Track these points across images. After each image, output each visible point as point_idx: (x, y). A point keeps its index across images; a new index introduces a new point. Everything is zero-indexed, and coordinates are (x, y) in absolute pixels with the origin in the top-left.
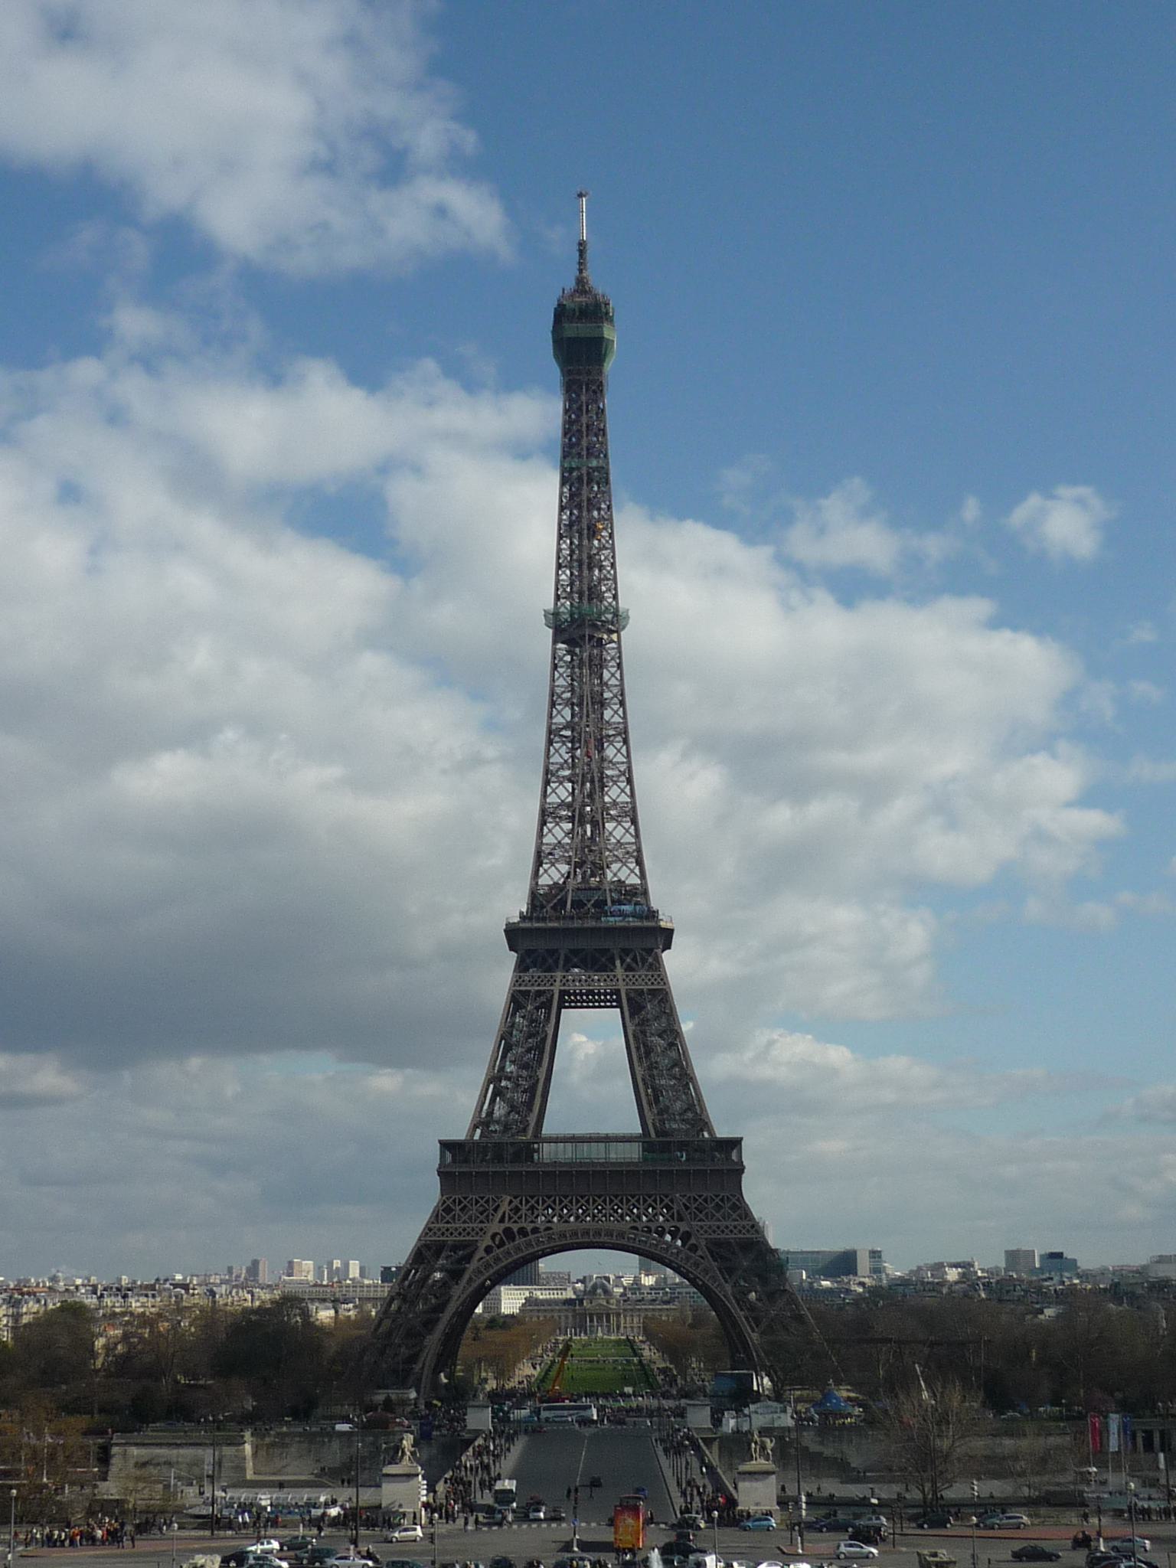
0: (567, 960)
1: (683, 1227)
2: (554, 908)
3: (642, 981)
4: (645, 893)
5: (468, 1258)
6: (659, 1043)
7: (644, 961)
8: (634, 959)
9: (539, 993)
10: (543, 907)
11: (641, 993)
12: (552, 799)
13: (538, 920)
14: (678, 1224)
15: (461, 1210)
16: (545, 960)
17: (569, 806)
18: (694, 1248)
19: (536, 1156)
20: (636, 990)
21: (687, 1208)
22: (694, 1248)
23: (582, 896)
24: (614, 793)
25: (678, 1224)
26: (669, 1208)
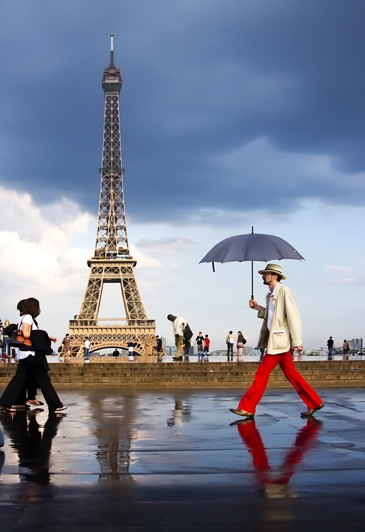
0: (105, 270)
1: (138, 343)
2: (102, 255)
3: (127, 276)
4: (128, 251)
5: (78, 351)
6: (132, 294)
7: (128, 271)
8: (125, 270)
9: (97, 279)
10: (98, 255)
11: (127, 279)
12: (102, 224)
13: (97, 259)
14: (137, 342)
15: (76, 338)
16: (99, 270)
17: (106, 226)
18: (141, 348)
19: (96, 324)
20: (125, 279)
21: (139, 338)
22: (141, 348)
23: (111, 252)
24: (120, 222)
25: (137, 342)
26: (134, 338)
